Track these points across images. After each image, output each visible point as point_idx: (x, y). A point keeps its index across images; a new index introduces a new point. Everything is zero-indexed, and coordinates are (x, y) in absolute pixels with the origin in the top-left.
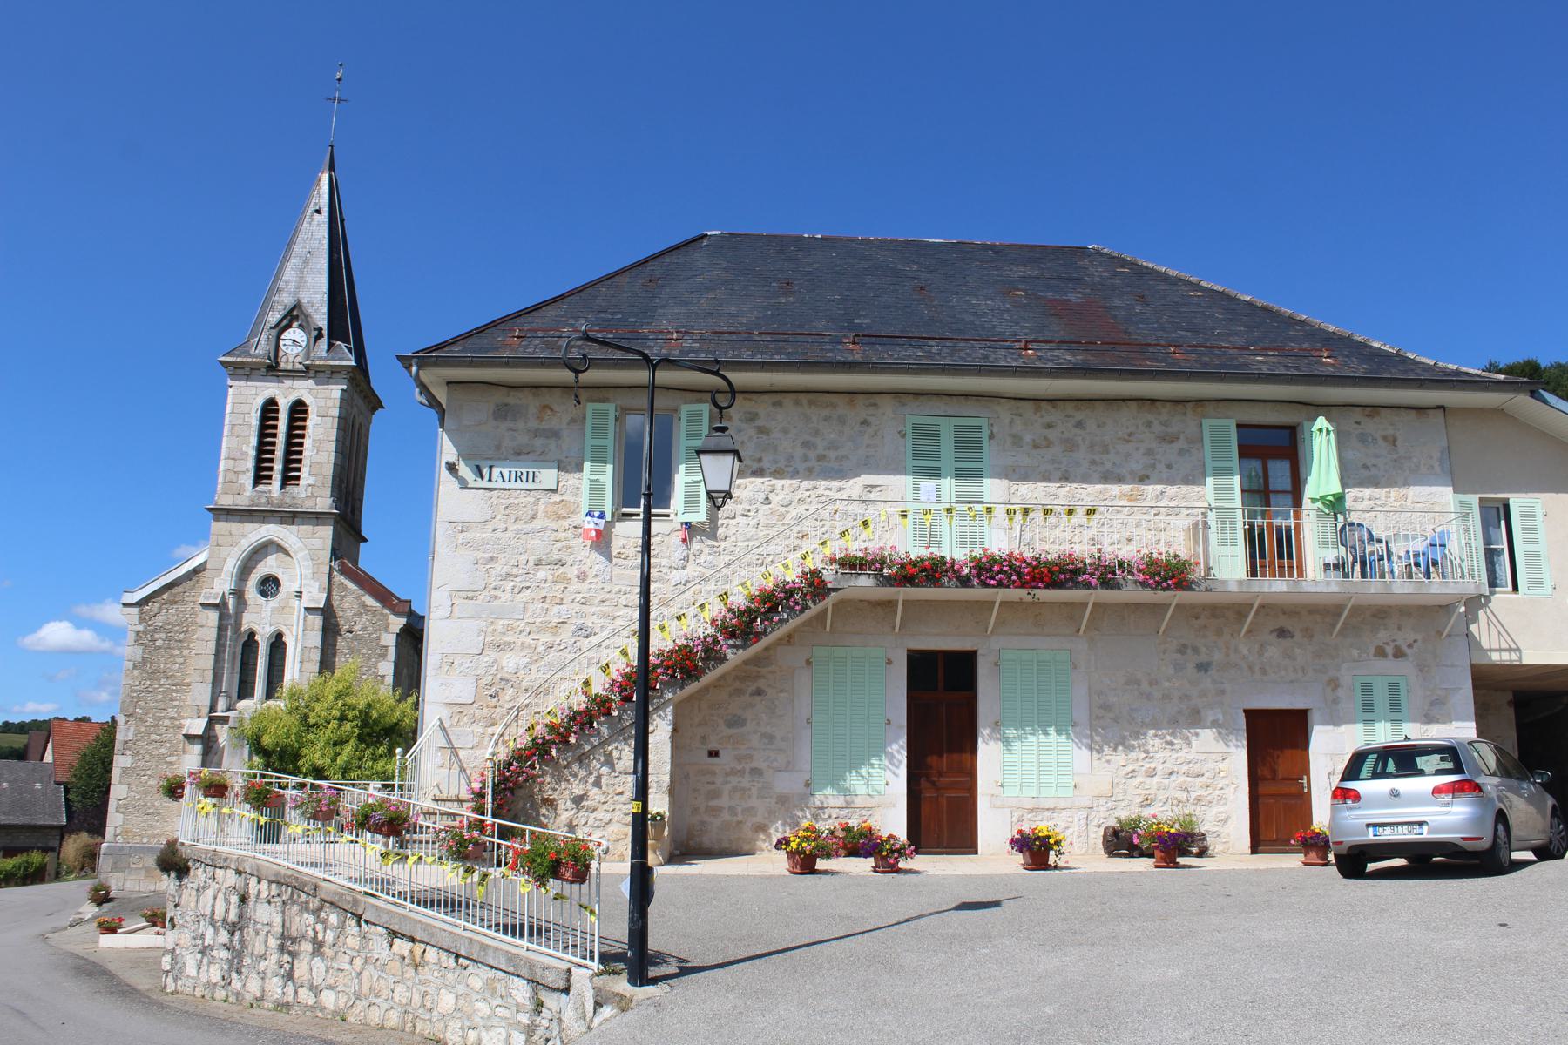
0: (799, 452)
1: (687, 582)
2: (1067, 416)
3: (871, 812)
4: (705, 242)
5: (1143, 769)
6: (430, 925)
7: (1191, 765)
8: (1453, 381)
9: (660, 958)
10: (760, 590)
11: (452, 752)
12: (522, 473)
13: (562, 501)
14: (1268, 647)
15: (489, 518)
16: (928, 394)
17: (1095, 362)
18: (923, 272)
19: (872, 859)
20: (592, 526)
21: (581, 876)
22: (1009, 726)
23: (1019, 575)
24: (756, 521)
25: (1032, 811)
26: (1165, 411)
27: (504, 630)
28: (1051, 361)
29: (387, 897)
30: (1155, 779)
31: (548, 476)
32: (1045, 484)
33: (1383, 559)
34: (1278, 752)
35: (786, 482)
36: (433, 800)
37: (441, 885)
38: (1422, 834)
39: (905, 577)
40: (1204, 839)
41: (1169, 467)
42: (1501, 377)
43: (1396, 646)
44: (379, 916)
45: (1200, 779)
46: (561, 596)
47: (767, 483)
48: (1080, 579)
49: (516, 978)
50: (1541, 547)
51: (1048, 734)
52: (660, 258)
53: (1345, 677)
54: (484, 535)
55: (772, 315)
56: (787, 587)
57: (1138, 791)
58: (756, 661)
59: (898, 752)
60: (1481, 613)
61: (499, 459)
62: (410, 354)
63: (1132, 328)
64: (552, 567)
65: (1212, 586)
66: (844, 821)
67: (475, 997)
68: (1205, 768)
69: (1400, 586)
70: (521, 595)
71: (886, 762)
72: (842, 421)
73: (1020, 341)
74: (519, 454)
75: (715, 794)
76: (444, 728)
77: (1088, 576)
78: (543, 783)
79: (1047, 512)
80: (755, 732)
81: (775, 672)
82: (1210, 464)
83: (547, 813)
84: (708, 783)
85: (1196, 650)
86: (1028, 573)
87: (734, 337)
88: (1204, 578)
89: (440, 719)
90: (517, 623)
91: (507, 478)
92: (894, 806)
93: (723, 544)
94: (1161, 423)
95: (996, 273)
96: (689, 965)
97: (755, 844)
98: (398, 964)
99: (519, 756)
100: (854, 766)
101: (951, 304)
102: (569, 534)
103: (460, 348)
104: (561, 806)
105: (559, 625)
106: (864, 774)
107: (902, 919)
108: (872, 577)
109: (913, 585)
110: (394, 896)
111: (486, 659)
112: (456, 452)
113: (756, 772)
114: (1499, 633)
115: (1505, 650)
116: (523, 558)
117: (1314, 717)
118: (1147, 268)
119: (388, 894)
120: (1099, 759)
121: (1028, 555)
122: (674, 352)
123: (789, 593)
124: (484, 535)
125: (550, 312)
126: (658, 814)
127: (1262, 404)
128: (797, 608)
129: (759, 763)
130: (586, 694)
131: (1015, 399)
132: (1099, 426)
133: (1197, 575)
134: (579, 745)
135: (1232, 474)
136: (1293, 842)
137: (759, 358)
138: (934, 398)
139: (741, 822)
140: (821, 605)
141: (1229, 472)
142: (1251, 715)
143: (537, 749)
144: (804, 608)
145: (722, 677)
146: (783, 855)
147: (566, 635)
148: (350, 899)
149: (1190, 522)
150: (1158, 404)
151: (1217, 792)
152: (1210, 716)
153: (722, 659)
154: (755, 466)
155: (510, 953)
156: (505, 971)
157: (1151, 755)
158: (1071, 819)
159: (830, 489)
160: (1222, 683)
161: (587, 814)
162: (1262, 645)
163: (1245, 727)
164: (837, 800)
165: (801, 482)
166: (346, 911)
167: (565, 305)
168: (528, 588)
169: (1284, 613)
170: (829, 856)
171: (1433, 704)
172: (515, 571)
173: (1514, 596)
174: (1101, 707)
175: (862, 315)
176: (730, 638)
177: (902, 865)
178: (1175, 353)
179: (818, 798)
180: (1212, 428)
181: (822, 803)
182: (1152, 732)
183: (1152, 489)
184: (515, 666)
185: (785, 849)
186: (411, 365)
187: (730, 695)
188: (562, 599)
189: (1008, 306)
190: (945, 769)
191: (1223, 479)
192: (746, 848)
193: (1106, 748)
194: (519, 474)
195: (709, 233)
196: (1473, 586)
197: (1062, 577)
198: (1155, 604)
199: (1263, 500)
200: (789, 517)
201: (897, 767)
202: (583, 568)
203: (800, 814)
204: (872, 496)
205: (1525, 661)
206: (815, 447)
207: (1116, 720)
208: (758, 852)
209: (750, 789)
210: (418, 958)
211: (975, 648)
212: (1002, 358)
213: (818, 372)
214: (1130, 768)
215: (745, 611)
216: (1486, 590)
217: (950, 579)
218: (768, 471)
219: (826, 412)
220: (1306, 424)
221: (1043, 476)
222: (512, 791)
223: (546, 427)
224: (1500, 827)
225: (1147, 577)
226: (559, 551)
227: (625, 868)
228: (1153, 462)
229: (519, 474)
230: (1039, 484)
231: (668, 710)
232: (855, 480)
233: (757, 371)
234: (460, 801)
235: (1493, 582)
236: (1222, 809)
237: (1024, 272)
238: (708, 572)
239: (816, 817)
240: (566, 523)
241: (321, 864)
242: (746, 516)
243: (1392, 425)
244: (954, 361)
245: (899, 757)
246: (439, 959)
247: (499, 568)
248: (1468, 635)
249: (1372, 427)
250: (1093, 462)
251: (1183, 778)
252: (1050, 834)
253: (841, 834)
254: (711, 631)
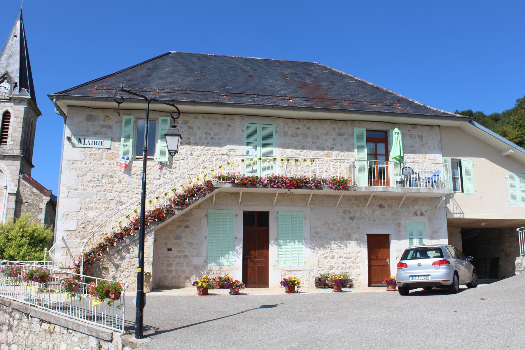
0: (204, 136)
1: (160, 184)
2: (304, 125)
3: (229, 272)
4: (170, 55)
5: (330, 256)
6: (57, 317)
7: (347, 254)
8: (443, 116)
9: (148, 328)
10: (188, 188)
11: (67, 249)
12: (97, 142)
13: (112, 153)
14: (376, 211)
15: (83, 158)
16: (253, 116)
17: (315, 106)
18: (252, 70)
19: (229, 289)
20: (124, 162)
21: (117, 296)
22: (280, 240)
23: (285, 183)
24: (187, 162)
25: (289, 271)
26: (340, 124)
27: (89, 202)
28: (299, 104)
29: (40, 306)
30: (334, 260)
31: (107, 143)
32: (296, 150)
33: (417, 180)
34: (378, 250)
35: (199, 147)
36: (59, 268)
37: (62, 301)
38: (429, 279)
39: (243, 184)
40: (352, 282)
41: (341, 145)
42: (459, 115)
43: (421, 212)
44: (36, 314)
45: (350, 259)
46: (112, 189)
47: (191, 148)
48: (308, 185)
49: (91, 337)
50: (472, 177)
51: (295, 243)
52: (152, 61)
53: (403, 223)
54: (82, 165)
55: (195, 84)
56: (198, 187)
57: (328, 264)
58: (186, 215)
59: (239, 249)
60: (451, 200)
61: (88, 136)
62: (53, 94)
63: (329, 93)
64: (108, 178)
65: (356, 189)
66: (219, 275)
67: (74, 345)
68: (352, 256)
69: (423, 190)
70: (96, 189)
71: (235, 253)
72: (220, 125)
73: (288, 97)
74: (96, 134)
75: (170, 265)
76: (64, 240)
77: (311, 184)
78: (103, 261)
79: (296, 160)
80: (185, 242)
81: (194, 219)
82: (356, 144)
83: (105, 273)
84: (167, 261)
85: (350, 212)
86: (289, 183)
87: (180, 92)
88: (353, 186)
89: (63, 236)
90: (94, 200)
91: (91, 143)
92: (238, 269)
93: (174, 170)
94: (338, 129)
95: (279, 71)
96: (159, 330)
97: (185, 284)
98: (44, 333)
99: (94, 251)
100: (223, 254)
101: (262, 82)
102: (115, 166)
103: (73, 93)
104: (110, 270)
105: (111, 200)
106: (226, 257)
107: (240, 312)
108: (230, 183)
109: (246, 187)
110: (42, 306)
111: (82, 213)
112: (71, 133)
113: (186, 256)
114: (457, 207)
115: (458, 213)
116: (97, 175)
117: (391, 237)
118: (335, 71)
119: (40, 305)
120: (314, 252)
121: (289, 176)
122: (157, 97)
123: (199, 189)
124: (82, 165)
125: (109, 80)
126: (148, 273)
127: (375, 123)
128: (202, 195)
129: (188, 254)
130: (121, 227)
131: (285, 118)
132: (316, 129)
133: (350, 185)
134: (118, 247)
135: (364, 148)
136: (383, 282)
137: (189, 100)
138: (255, 117)
139: (180, 276)
140: (211, 194)
141: (363, 147)
142: (368, 235)
143: (101, 248)
144: (205, 195)
145: (173, 221)
146: (195, 288)
147: (113, 204)
148: (24, 308)
149: (348, 165)
150: (338, 122)
151: (357, 264)
152: (354, 236)
153: (173, 214)
154: (187, 141)
155: (89, 327)
156: (87, 334)
157: (333, 251)
158: (303, 274)
159: (215, 150)
160: (359, 224)
161: (120, 273)
162: (373, 211)
163: (367, 241)
164: (216, 267)
165: (204, 147)
166: (23, 312)
167: (115, 78)
168: (98, 186)
169: (382, 199)
170: (213, 288)
171: (433, 232)
172: (94, 179)
173: (462, 194)
174: (315, 233)
175: (229, 85)
176: (176, 206)
177: (240, 291)
178: (344, 103)
179: (209, 266)
180: (357, 131)
181: (211, 268)
182: (333, 242)
183: (335, 153)
184: (93, 216)
185: (197, 286)
186: (53, 99)
187: (176, 228)
188: (112, 190)
189: (283, 83)
190: (257, 256)
191: (361, 150)
192: (182, 285)
193: (316, 248)
194: (96, 142)
195: (172, 52)
196: (448, 190)
197: (301, 184)
198: (335, 195)
199: (375, 158)
200: (200, 160)
201: (239, 255)
202: (120, 179)
203: (202, 272)
204: (231, 153)
205: (465, 217)
206: (210, 134)
207: (320, 238)
208: (186, 287)
209: (183, 263)
210: (52, 330)
211: (269, 211)
212: (281, 103)
213: (212, 106)
214: (325, 255)
215: (182, 196)
216: (452, 192)
217: (260, 185)
218: (192, 143)
219: (214, 121)
220: (391, 130)
221: (295, 147)
222: (91, 264)
223: (107, 124)
224: (456, 276)
225: (332, 185)
226: (111, 172)
227: (135, 293)
228: (335, 143)
229: (96, 142)
230: (293, 150)
231: (152, 233)
232: (225, 147)
233: (189, 105)
234: (70, 268)
235: (455, 189)
236: (358, 270)
237: (290, 71)
238: (168, 181)
239: (208, 274)
240: (114, 161)
241: (13, 294)
242: (183, 160)
243: (421, 131)
244: (263, 103)
245: (240, 251)
246: (60, 330)
247: (87, 178)
248: (446, 208)
249: (415, 132)
250: (313, 142)
251: (344, 259)
252: (295, 280)
253: (218, 280)
254: (169, 203)
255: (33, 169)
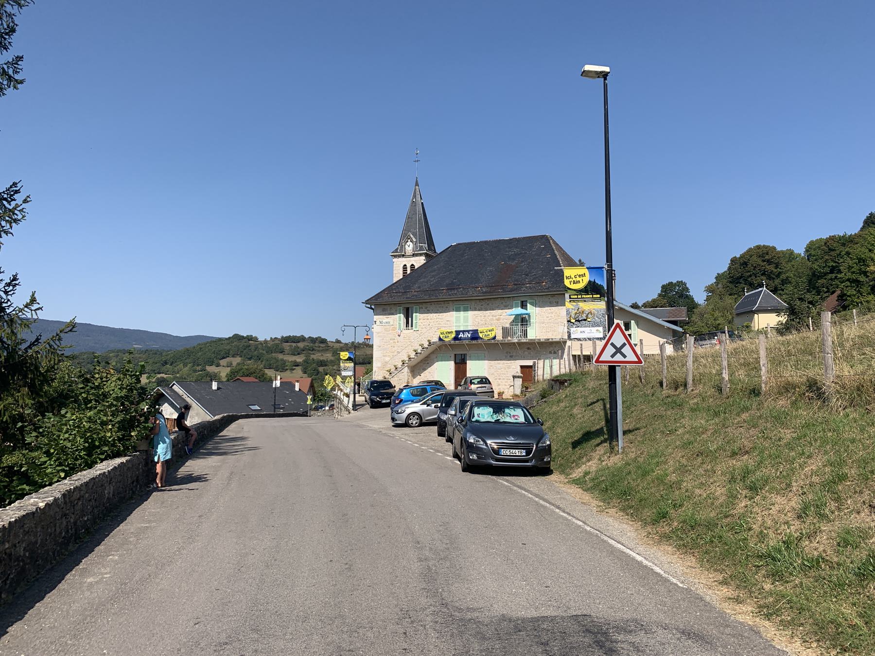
72: (443, 307)
85: (510, 353)
255: (400, 318)
